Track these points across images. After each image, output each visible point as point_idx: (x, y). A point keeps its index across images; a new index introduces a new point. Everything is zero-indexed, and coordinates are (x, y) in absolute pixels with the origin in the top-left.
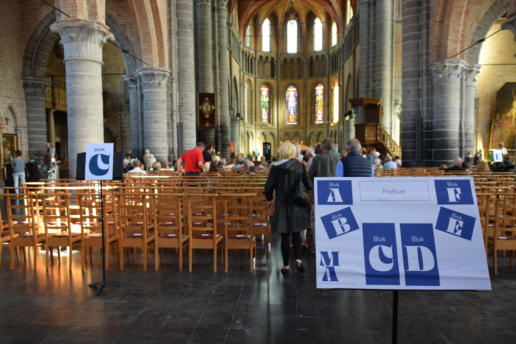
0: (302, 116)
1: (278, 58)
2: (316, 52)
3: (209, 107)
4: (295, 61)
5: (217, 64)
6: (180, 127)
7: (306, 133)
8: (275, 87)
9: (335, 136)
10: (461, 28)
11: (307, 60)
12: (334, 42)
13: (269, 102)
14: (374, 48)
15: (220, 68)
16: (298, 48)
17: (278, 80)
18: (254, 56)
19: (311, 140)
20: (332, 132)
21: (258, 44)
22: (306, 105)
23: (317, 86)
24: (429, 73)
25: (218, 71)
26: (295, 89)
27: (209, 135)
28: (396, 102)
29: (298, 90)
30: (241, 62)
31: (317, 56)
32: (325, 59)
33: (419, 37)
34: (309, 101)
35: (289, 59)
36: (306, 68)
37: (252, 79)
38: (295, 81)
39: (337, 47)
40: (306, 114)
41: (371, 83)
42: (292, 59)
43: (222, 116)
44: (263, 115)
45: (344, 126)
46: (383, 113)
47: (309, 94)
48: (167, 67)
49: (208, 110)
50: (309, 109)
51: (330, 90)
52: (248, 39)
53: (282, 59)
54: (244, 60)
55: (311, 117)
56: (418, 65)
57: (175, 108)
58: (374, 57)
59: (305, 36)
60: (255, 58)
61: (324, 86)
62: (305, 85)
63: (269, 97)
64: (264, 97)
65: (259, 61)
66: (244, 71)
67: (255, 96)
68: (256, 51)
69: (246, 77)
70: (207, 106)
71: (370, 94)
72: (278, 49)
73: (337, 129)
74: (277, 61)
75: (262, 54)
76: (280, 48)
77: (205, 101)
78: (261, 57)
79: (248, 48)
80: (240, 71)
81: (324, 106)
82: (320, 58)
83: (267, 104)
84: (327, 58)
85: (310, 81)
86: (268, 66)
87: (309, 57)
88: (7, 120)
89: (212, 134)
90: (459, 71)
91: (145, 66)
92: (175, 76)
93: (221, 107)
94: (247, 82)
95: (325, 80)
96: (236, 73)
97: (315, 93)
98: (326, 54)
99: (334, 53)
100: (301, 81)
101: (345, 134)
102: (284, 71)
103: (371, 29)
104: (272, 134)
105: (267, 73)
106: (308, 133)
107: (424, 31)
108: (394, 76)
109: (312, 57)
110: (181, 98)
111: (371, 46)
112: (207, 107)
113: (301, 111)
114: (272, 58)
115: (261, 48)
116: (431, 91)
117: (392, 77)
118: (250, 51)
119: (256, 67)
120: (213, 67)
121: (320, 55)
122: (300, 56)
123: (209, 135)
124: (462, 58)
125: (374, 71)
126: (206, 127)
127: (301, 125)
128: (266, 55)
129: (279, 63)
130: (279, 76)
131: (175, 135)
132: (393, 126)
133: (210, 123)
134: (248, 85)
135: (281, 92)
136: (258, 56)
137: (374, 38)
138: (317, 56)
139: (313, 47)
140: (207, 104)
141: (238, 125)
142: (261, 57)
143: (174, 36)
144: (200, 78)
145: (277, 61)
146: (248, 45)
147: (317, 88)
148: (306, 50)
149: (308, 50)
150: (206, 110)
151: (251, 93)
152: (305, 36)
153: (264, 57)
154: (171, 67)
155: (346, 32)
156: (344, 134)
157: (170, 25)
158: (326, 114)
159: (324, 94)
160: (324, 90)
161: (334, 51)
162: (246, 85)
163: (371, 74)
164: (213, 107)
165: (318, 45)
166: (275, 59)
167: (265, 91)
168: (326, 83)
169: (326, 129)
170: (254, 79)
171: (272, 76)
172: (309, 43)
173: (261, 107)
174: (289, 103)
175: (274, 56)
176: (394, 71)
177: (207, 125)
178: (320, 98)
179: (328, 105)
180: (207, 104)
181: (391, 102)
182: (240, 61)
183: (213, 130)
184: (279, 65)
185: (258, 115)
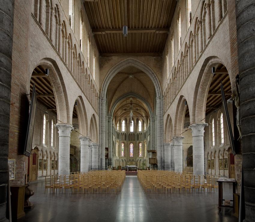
2: (139, 132)
4: (133, 134)
5: (109, 138)
6: (101, 159)
10: (170, 135)
14: (154, 135)
15: (110, 140)
23: (140, 143)
24: (163, 146)
25: (109, 141)
29: (134, 145)
31: (140, 133)
33: (161, 136)
34: (137, 149)
35: (131, 134)
36: (136, 137)
41: (153, 145)
42: (132, 134)
48: (98, 143)
50: (137, 151)
52: (118, 127)
53: (129, 134)
55: (138, 154)
56: (161, 143)
57: (100, 154)
58: (154, 137)
71: (153, 149)
83: (123, 150)
85: (138, 142)
86: (124, 136)
87: (137, 134)
88: (53, 156)
90: (170, 146)
91: (93, 143)
92: (100, 145)
95: (142, 141)
96: (114, 140)
100: (135, 142)
102: (129, 138)
103: (153, 129)
104: (125, 160)
106: (137, 160)
107: (162, 135)
109: (138, 133)
110: (102, 151)
111: (153, 134)
113: (135, 152)
116: (164, 150)
122: (134, 133)
124: (171, 142)
125: (154, 142)
131: (100, 161)
136: (121, 133)
137: (154, 132)
139: (138, 130)
143: (100, 134)
146: (118, 129)
154: (99, 143)
155: (148, 127)
157: (99, 132)
158: (143, 153)
159: (142, 146)
160: (142, 145)
163: (153, 143)
167: (123, 145)
171: (125, 140)
175: (126, 133)
178: (140, 148)
183: (108, 159)
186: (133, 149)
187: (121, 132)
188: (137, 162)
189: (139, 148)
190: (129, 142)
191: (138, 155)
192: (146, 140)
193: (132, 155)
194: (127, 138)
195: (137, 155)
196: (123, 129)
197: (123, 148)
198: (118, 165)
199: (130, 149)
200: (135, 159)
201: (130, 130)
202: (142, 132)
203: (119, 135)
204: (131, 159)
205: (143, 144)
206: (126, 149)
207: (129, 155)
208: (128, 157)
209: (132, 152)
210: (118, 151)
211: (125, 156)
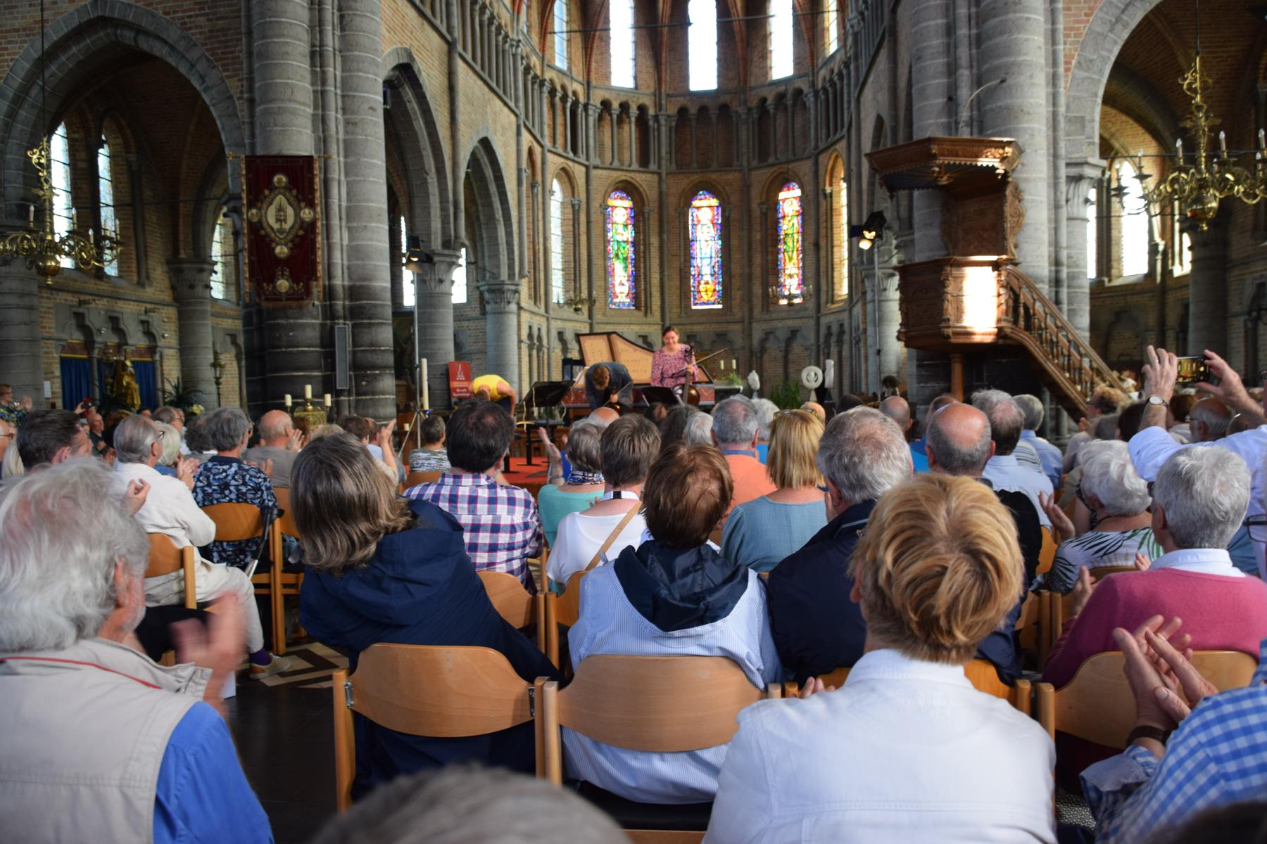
0: (736, 283)
1: (659, 106)
3: (290, 211)
4: (713, 113)
7: (750, 335)
8: (651, 193)
9: (840, 342)
11: (749, 109)
12: (832, 44)
13: (635, 244)
16: (719, 76)
17: (659, 174)
18: (582, 100)
19: (766, 357)
20: (829, 328)
21: (593, 65)
22: (750, 248)
26: (715, 202)
27: (292, 328)
28: (1074, 171)
29: (724, 206)
30: (521, 104)
32: (804, 104)
34: (757, 236)
35: (693, 110)
37: (579, 172)
38: (714, 176)
39: (838, 57)
40: (750, 276)
43: (355, 252)
44: (617, 283)
45: (865, 304)
46: (1020, 215)
47: (756, 213)
49: (287, 226)
50: (758, 259)
51: (821, 197)
53: (673, 110)
54: (559, 120)
55: (765, 285)
60: (586, 106)
61: (801, 187)
62: (746, 187)
63: (635, 227)
64: (620, 228)
65: (600, 118)
66: (547, 143)
67: (588, 222)
68: (588, 86)
69: (554, 162)
70: (280, 209)
72: (659, 81)
73: (845, 315)
75: (607, 95)
76: (666, 76)
77: (272, 188)
78: (606, 104)
79: (560, 71)
80: (519, 134)
81: (803, 251)
82: (790, 103)
83: (628, 251)
85: (760, 177)
86: (630, 131)
87: (754, 103)
89: (309, 325)
93: (352, 214)
94: (558, 177)
95: (805, 167)
97: (776, 210)
98: (806, 88)
99: (831, 80)
100: (733, 177)
101: (870, 330)
102: (678, 148)
106: (757, 336)
108: (1061, 60)
109: (764, 100)
112: (279, 215)
113: (736, 269)
114: (642, 109)
115: (607, 76)
117: (1055, 64)
118: (567, 82)
120: (312, 54)
122: (725, 99)
123: (292, 328)
126: (276, 296)
127: (736, 310)
128: (624, 99)
129: (663, 122)
130: (663, 162)
132: (1064, 273)
133: (294, 279)
135: (671, 211)
136: (596, 100)
138: (781, 97)
139: (766, 69)
140: (280, 199)
141: (513, 307)
142: (606, 104)
144: (257, 98)
145: (656, 118)
146: (560, 63)
147: (782, 195)
148: (745, 81)
149: (753, 82)
150: (276, 226)
151: (576, 213)
153: (615, 105)
156: (865, 330)
158: (811, 274)
159: (803, 214)
160: (803, 200)
161: (832, 71)
162: (556, 185)
164: (307, 214)
165: (782, 61)
166: (651, 112)
167: (621, 209)
168: (808, 178)
169: (812, 322)
170: (584, 169)
171: (644, 161)
172: (755, 59)
174: (697, 245)
175: (648, 101)
176: (1060, 37)
177: (283, 284)
179: (817, 245)
180: (280, 199)
181: (1055, 168)
182: (517, 101)
184: (663, 129)
188: (763, 350)
189: (776, 223)
191: (766, 295)
192: (841, 146)
193: (707, 291)
195: (757, 290)
196: (622, 66)
198: (535, 379)
199: (687, 244)
200: (737, 327)
201: (685, 78)
202: (804, 85)
203: (574, 116)
204: (697, 328)
205: (810, 188)
206: (654, 241)
207: (685, 293)
208: (673, 313)
209: (706, 271)
210: (576, 260)
211: (640, 299)
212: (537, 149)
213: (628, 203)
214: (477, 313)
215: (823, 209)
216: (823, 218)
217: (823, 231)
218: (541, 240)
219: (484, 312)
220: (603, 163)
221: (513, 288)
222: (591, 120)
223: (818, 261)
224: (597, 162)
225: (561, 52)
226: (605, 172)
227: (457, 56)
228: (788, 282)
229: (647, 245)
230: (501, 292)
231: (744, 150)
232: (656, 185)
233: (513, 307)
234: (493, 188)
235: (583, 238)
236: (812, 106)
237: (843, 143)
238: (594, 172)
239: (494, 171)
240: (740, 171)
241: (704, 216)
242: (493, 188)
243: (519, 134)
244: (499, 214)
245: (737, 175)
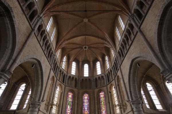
1: (79, 78)
11: (94, 80)
26: (88, 95)
29: (89, 96)
31: (99, 77)
35: (84, 79)
36: (93, 84)
38: (88, 90)
40: (95, 109)
42: (86, 80)
47: (96, 97)
53: (81, 79)
59: (93, 69)
61: (104, 92)
66: (58, 78)
67: (64, 96)
68: (67, 73)
72: (79, 74)
74: (78, 80)
75: (70, 75)
80: (51, 70)
81: (106, 104)
82: (101, 78)
83: (71, 103)
84: (105, 77)
85: (96, 90)
87: (95, 78)
95: (105, 88)
98: (103, 75)
105: (72, 86)
113: (92, 108)
114: (76, 79)
119: (67, 80)
121: (100, 76)
122: (90, 78)
129: (79, 80)
134: (60, 89)
138: (99, 77)
145: (78, 80)
147: (100, 94)
149: (94, 75)
151: (61, 94)
152: (93, 69)
153: (72, 77)
158: (108, 109)
159: (105, 97)
161: (109, 71)
165: (99, 72)
166: (77, 79)
171: (76, 86)
172: (95, 72)
173: (66, 104)
174: (84, 103)
175: (77, 77)
178: (102, 99)
179: (109, 103)
182: (52, 64)
185: (64, 110)
186: (88, 103)
187: (69, 75)
189: (100, 99)
190: (81, 91)
194: (79, 85)
196: (73, 72)
197: (70, 100)
199: (83, 102)
201: (83, 74)
202: (103, 75)
206: (76, 102)
209: (86, 108)
212: (55, 78)
213: (72, 94)
214: (26, 111)
215: (109, 95)
216: (110, 97)
217: (110, 100)
218: (52, 96)
219: (28, 111)
220: (68, 85)
221: (38, 103)
222: (67, 78)
223: (110, 106)
224: (67, 85)
225: (64, 66)
226: (68, 87)
227: (33, 33)
228: (103, 111)
229: (75, 102)
230: (35, 104)
231: (93, 86)
232: (77, 91)
233: (37, 110)
234: (40, 76)
235: (62, 99)
236: (105, 78)
237: (114, 80)
238: (66, 87)
239: (41, 72)
240: (92, 89)
241: (86, 97)
242: (40, 76)
243: (51, 70)
244: (40, 83)
245: (92, 90)
